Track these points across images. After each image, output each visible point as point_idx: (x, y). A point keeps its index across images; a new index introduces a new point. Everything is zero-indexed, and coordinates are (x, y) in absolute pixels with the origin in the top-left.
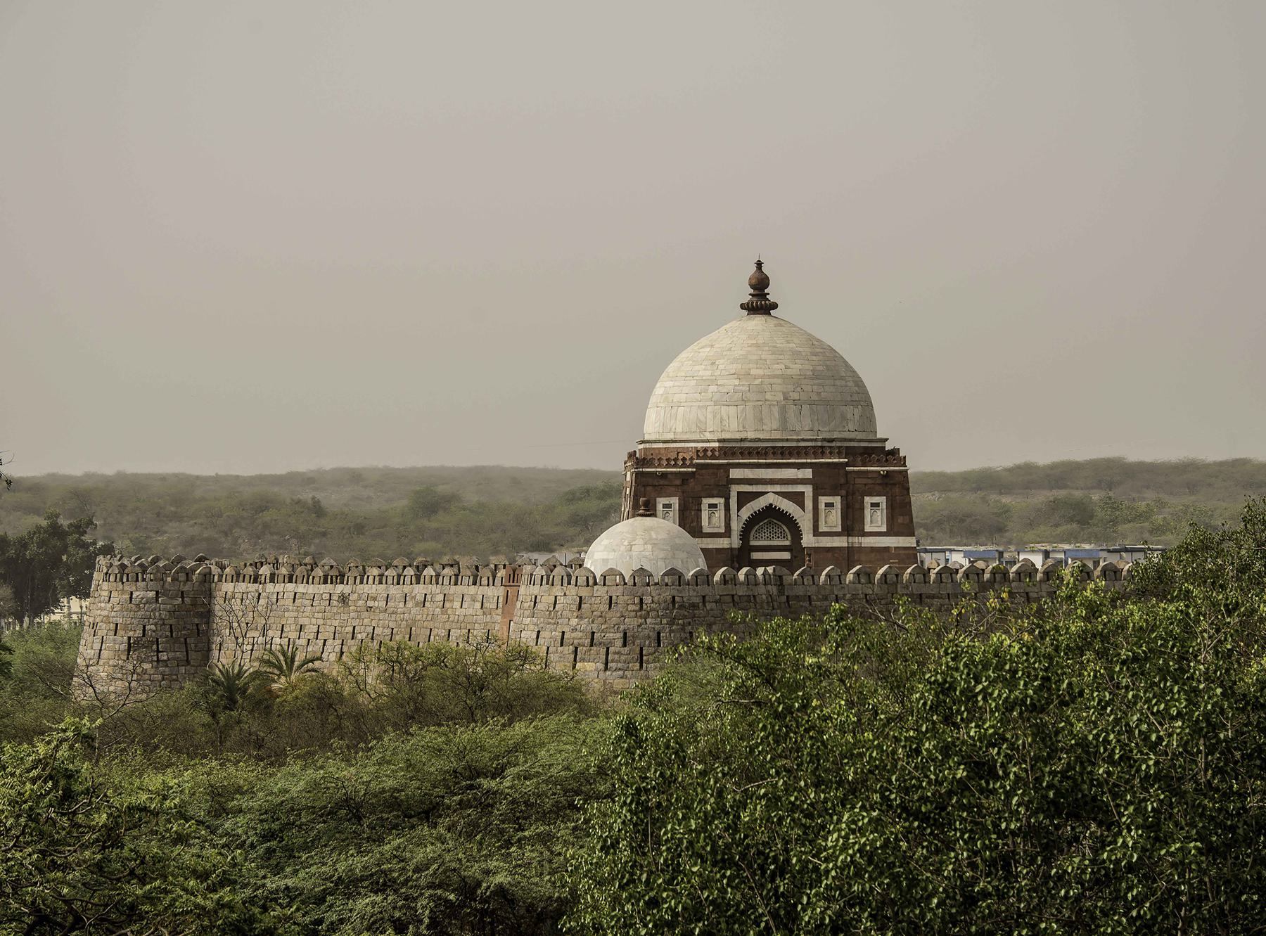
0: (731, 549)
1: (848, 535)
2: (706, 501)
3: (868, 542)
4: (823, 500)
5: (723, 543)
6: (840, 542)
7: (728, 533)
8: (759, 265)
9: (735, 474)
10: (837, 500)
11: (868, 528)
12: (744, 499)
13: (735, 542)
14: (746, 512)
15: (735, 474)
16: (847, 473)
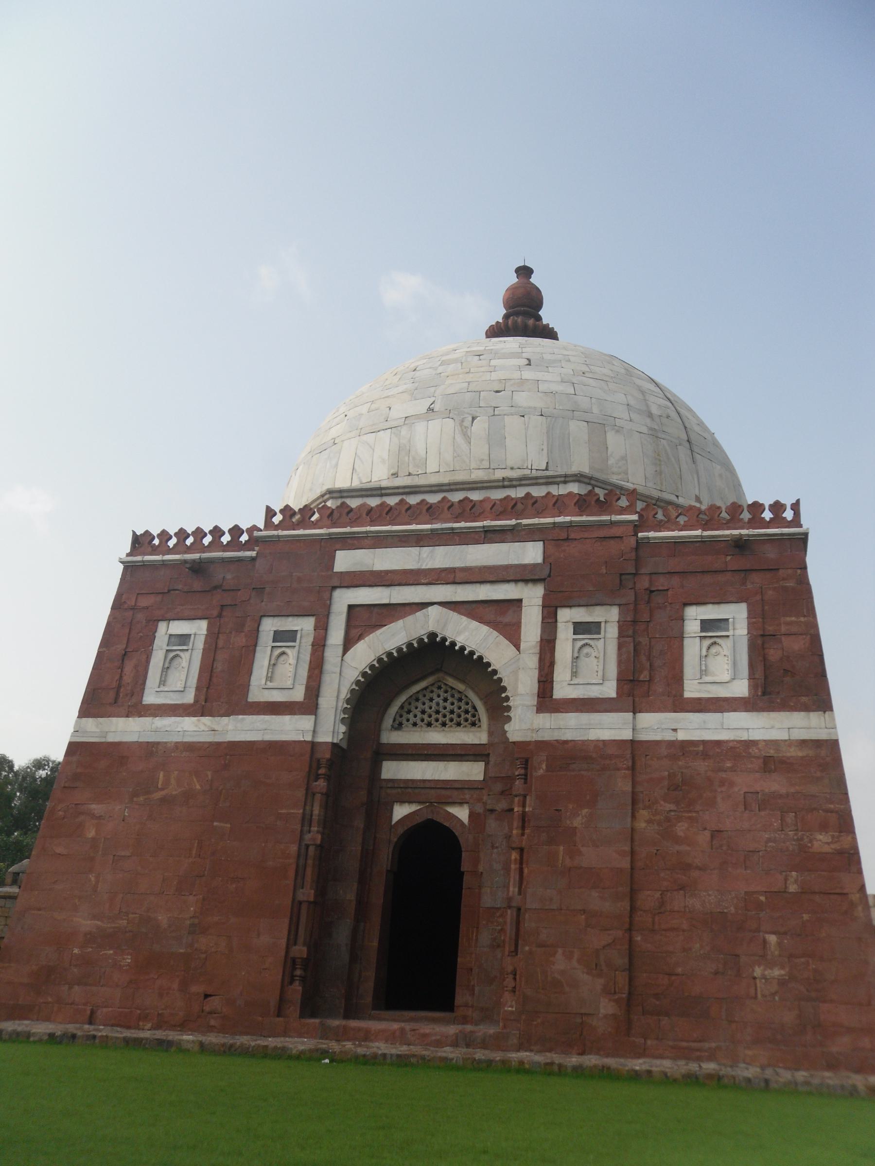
0: (313, 745)
1: (635, 710)
2: (269, 626)
3: (693, 727)
4: (566, 616)
5: (292, 729)
6: (612, 727)
7: (309, 705)
8: (524, 272)
9: (345, 561)
10: (609, 617)
11: (692, 690)
12: (364, 621)
13: (328, 727)
14: (367, 653)
15: (345, 561)
16: (640, 545)
